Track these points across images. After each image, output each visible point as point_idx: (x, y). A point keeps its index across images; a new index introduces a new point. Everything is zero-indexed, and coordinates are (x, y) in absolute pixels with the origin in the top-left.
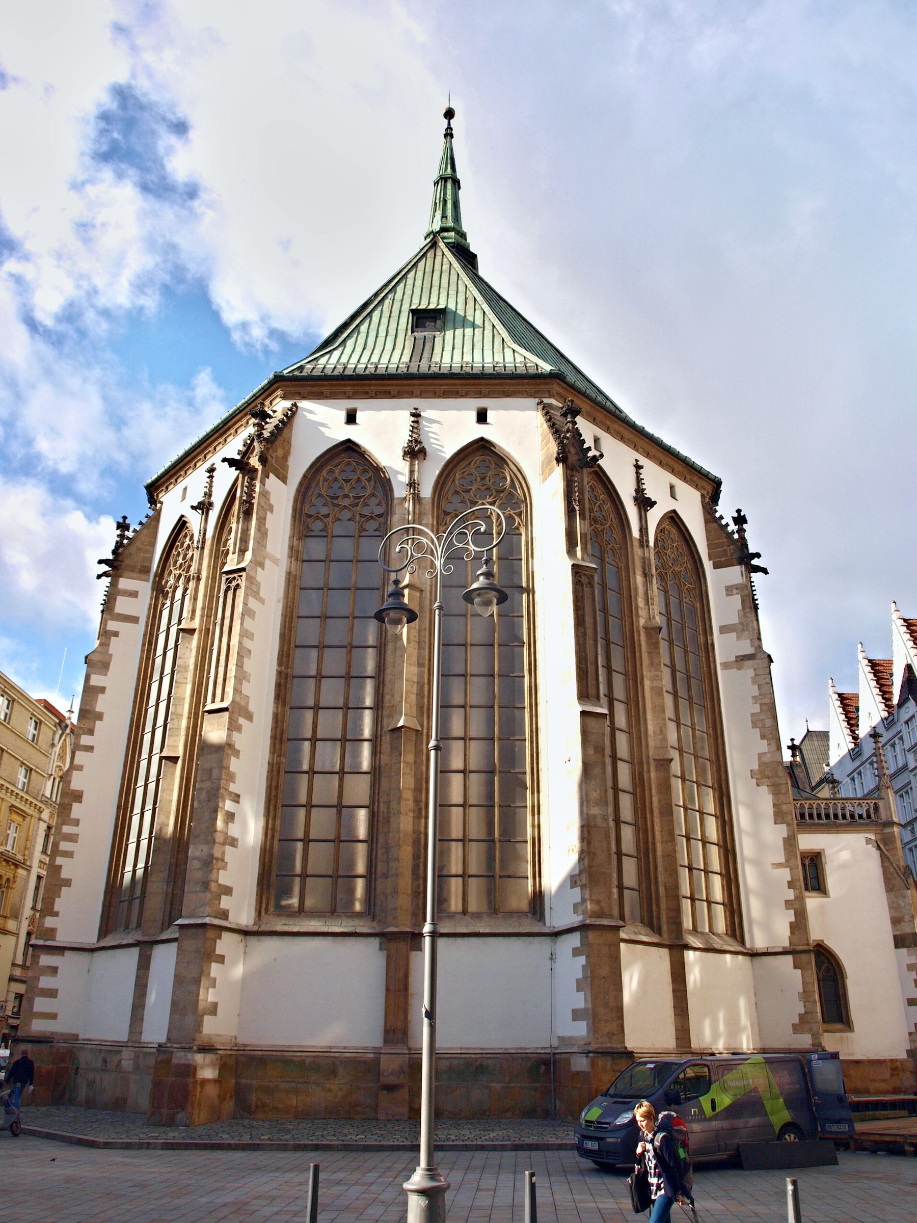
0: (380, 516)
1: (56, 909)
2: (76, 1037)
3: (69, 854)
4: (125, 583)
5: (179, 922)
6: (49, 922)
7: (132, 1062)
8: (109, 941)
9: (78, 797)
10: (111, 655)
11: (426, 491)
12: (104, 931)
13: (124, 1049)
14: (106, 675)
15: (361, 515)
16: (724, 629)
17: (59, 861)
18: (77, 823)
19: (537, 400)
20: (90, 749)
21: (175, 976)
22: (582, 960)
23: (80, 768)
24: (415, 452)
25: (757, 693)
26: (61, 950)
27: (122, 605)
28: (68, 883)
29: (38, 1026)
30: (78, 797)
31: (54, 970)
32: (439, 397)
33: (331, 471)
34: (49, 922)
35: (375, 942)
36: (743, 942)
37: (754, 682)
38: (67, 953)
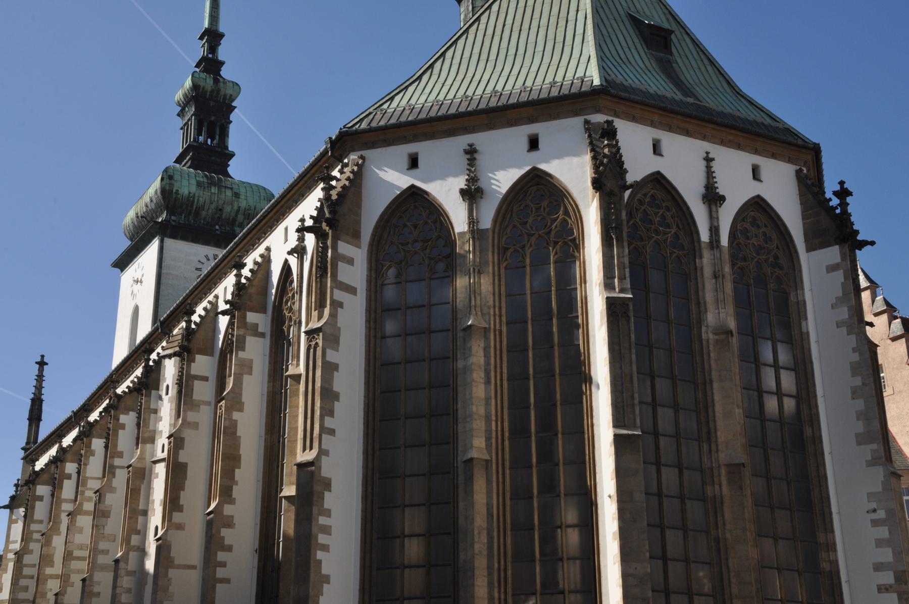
10: (339, 329)
11: (724, 241)
18: (328, 513)
20: (332, 432)
28: (326, 579)
32: (725, 145)
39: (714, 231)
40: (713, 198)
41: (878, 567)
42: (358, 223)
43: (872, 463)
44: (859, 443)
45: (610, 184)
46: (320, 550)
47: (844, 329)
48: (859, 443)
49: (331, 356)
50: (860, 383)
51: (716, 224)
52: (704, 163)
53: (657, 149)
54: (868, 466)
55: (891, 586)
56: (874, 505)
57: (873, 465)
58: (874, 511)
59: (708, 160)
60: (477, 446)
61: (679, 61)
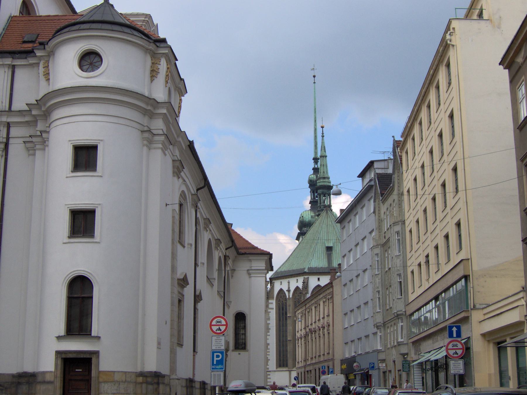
4: (270, 301)
6: (268, 367)
8: (279, 369)
9: (268, 344)
12: (277, 368)
26: (270, 371)
27: (270, 306)
30: (268, 344)
34: (268, 367)
49: (268, 322)
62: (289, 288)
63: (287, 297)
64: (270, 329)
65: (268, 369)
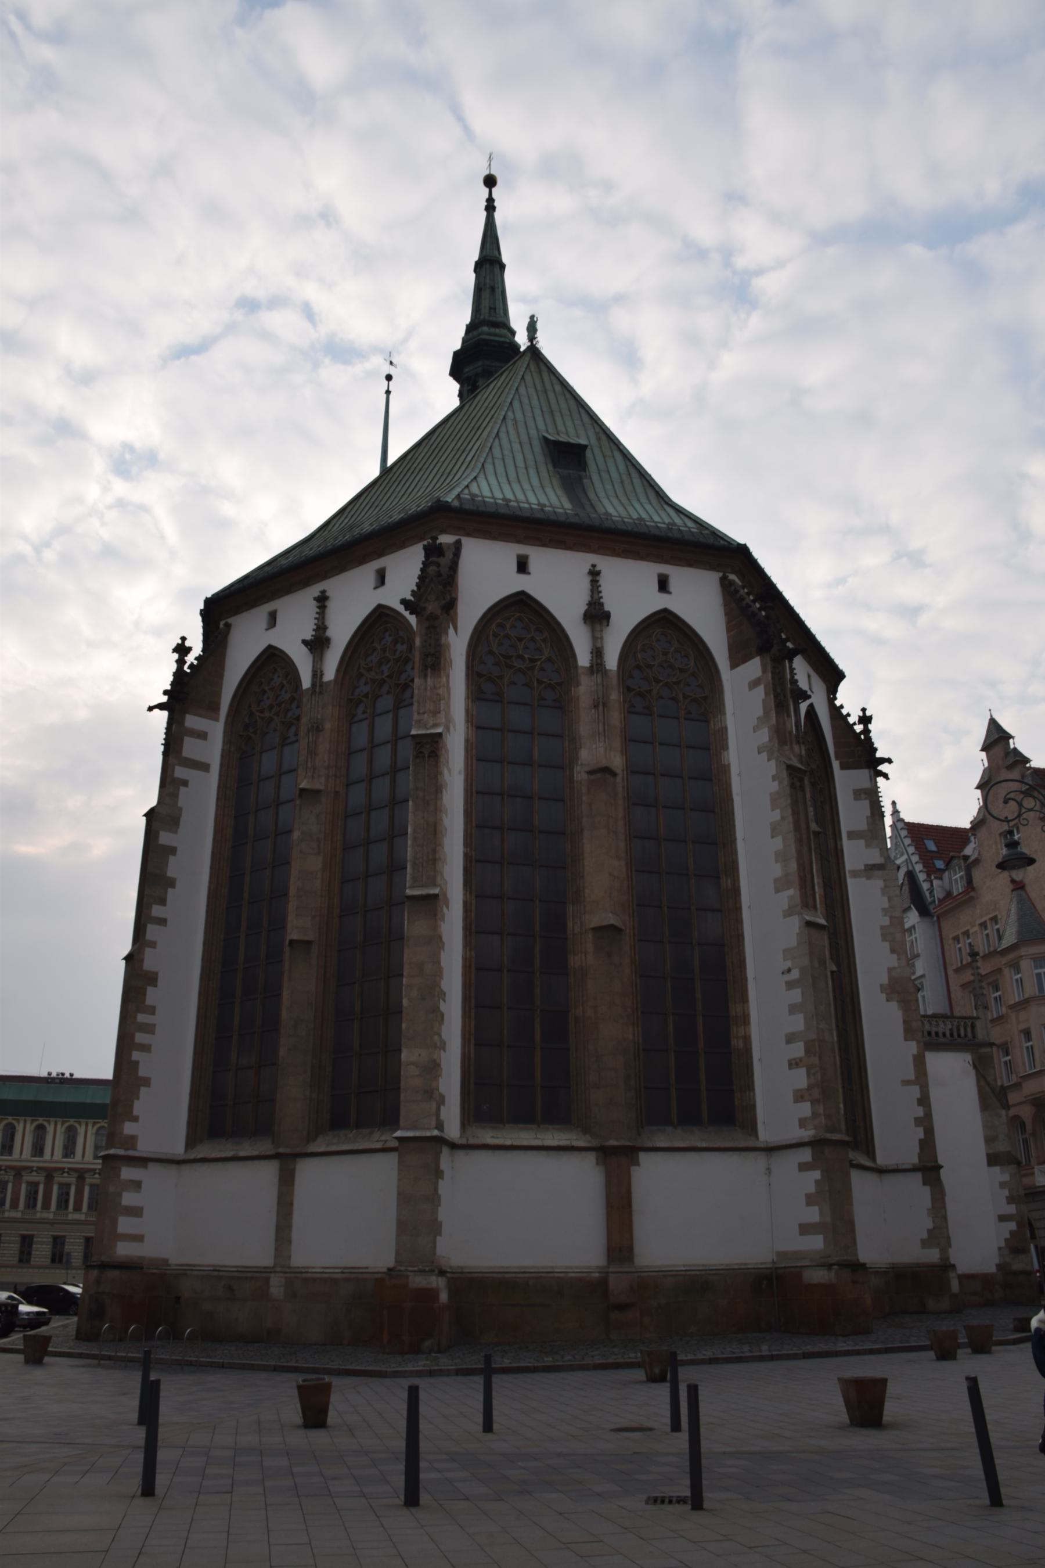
0: (560, 684)
1: (136, 1111)
2: (165, 1262)
3: (145, 1048)
4: (192, 721)
5: (399, 1134)
6: (129, 1128)
7: (282, 1289)
8: (204, 1150)
9: (152, 979)
10: (181, 809)
11: (612, 661)
12: (191, 1142)
13: (272, 1275)
14: (176, 832)
15: (540, 682)
16: (852, 835)
17: (136, 1055)
18: (152, 1010)
19: (721, 574)
20: (162, 922)
21: (399, 1194)
22: (817, 1175)
23: (153, 945)
24: (596, 615)
25: (887, 905)
26: (143, 1161)
27: (191, 748)
28: (146, 1082)
29: (124, 1250)
30: (152, 979)
31: (137, 1185)
33: (501, 626)
34: (129, 1128)
35: (591, 1158)
36: (873, 1158)
37: (883, 894)
38: (150, 1165)
39: (598, 653)
40: (596, 615)
41: (790, 1039)
42: (218, 695)
43: (788, 914)
44: (777, 890)
45: (432, 607)
46: (137, 1050)
47: (765, 755)
48: (777, 890)
50: (779, 817)
51: (599, 645)
52: (589, 578)
53: (522, 566)
54: (785, 917)
55: (801, 1060)
56: (789, 964)
57: (789, 915)
58: (789, 971)
59: (594, 574)
60: (299, 925)
61: (595, 478)
62: (321, 627)
63: (306, 683)
64: (172, 883)
65: (131, 1141)
